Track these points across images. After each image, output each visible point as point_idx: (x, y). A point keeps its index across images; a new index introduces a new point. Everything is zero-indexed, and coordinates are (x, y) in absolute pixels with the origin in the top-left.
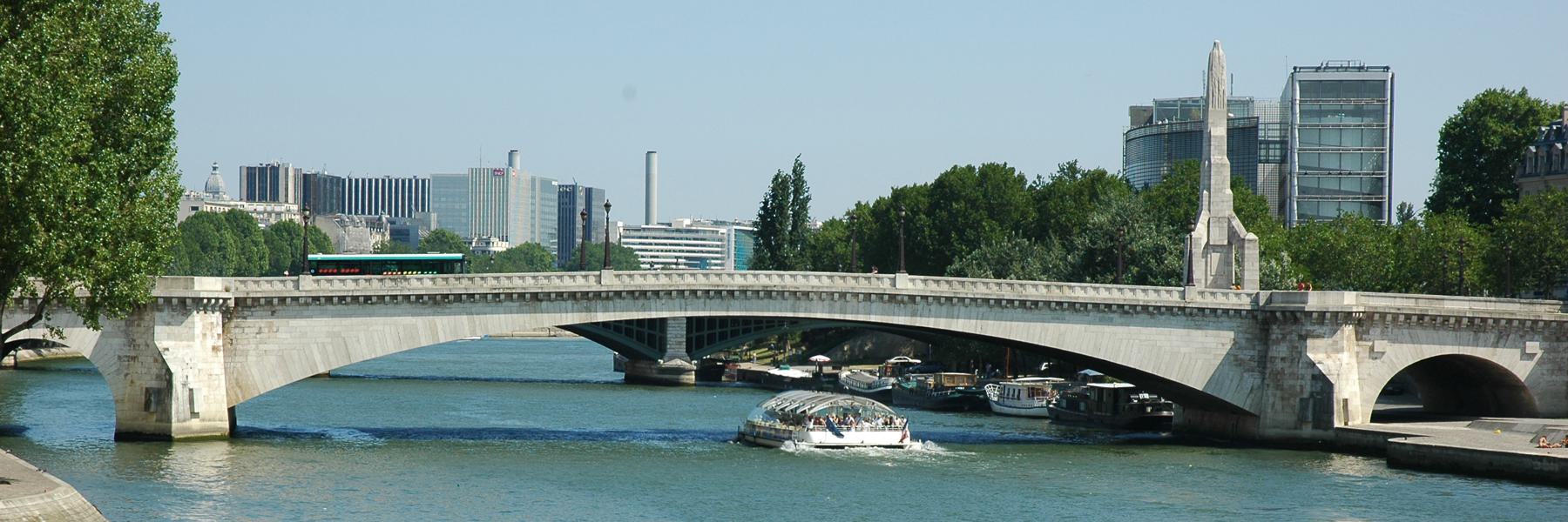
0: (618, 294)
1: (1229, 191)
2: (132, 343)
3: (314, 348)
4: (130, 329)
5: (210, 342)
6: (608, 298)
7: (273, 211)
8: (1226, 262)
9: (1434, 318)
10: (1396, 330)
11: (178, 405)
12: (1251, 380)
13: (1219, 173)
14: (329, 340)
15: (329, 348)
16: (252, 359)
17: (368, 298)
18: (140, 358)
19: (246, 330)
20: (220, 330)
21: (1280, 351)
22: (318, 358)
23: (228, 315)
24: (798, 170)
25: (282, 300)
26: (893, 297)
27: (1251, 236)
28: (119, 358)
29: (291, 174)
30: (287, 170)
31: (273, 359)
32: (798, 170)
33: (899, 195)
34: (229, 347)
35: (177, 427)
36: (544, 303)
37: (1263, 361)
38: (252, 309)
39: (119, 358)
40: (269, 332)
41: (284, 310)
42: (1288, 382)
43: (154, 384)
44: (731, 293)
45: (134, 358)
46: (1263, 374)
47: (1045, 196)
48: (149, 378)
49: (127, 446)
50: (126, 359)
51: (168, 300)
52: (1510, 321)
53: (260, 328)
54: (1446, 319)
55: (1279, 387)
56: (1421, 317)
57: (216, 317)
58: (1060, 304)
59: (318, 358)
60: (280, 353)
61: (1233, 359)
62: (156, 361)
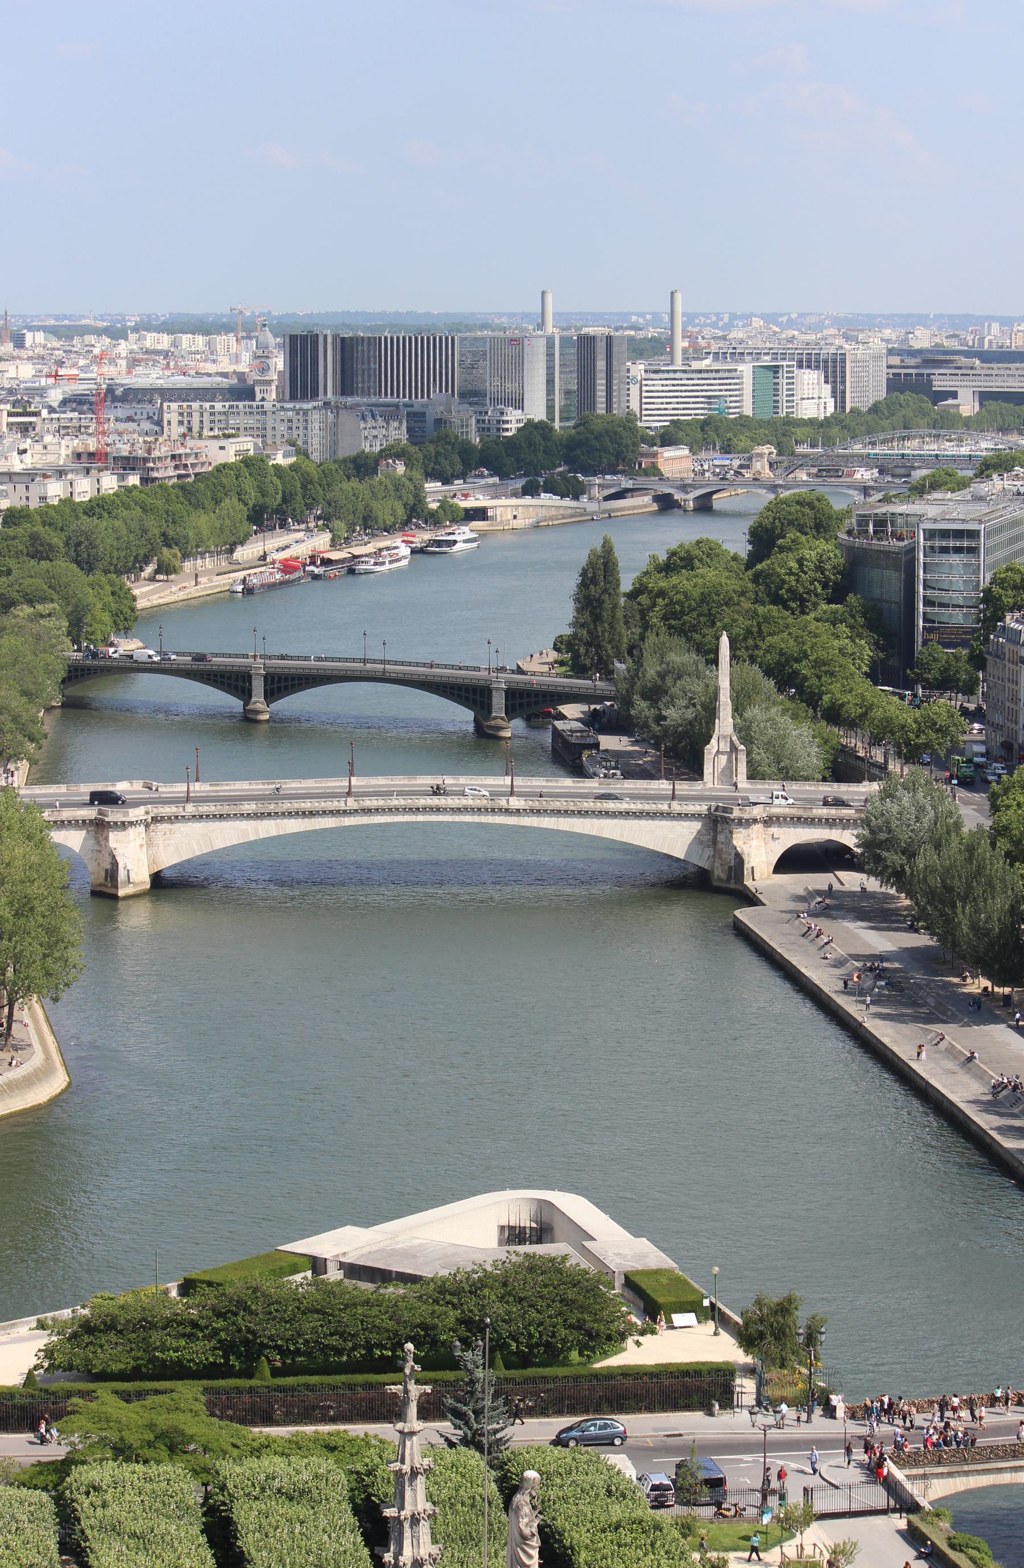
0: (356, 811)
1: (731, 720)
2: (98, 843)
5: (138, 843)
7: (301, 409)
8: (729, 761)
9: (806, 819)
11: (122, 875)
12: (708, 852)
13: (724, 709)
16: (161, 848)
17: (221, 815)
20: (144, 835)
21: (721, 838)
22: (196, 847)
23: (147, 826)
25: (177, 817)
26: (507, 810)
27: (742, 747)
29: (329, 340)
30: (325, 337)
34: (150, 843)
35: (121, 893)
37: (715, 842)
42: (724, 856)
43: (109, 867)
44: (418, 809)
46: (715, 848)
49: (97, 900)
51: (116, 823)
52: (848, 820)
54: (813, 819)
55: (720, 858)
56: (799, 819)
57: (142, 828)
58: (600, 812)
59: (196, 847)
61: (698, 840)
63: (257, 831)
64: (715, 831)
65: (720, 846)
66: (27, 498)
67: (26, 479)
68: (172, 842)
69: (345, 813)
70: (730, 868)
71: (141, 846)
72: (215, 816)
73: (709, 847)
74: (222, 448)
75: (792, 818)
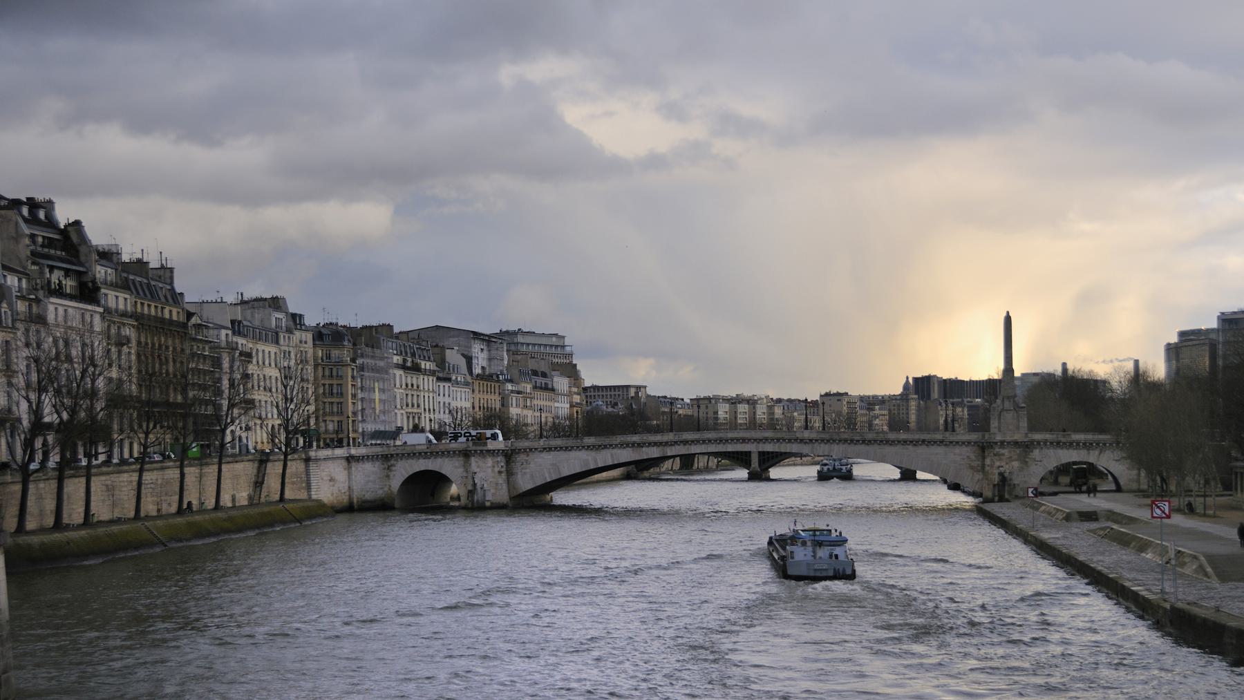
5: (497, 469)
6: (671, 445)
9: (1064, 443)
10: (1046, 450)
12: (979, 476)
15: (552, 471)
16: (519, 476)
17: (567, 448)
22: (547, 475)
34: (510, 473)
36: (644, 449)
37: (983, 466)
56: (1058, 443)
59: (547, 475)
63: (596, 461)
64: (984, 458)
65: (987, 468)
66: (707, 413)
67: (706, 402)
68: (528, 470)
69: (666, 444)
70: (994, 485)
71: (500, 472)
72: (561, 448)
73: (979, 471)
74: (838, 400)
75: (1051, 443)
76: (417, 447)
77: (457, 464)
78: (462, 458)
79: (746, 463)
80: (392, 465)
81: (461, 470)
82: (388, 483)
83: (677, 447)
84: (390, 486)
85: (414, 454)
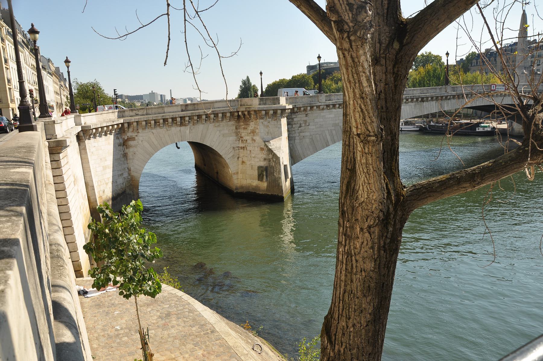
3: (327, 132)
4: (239, 130)
14: (333, 128)
15: (334, 132)
18: (248, 148)
19: (294, 126)
24: (248, 77)
28: (234, 148)
31: (307, 140)
32: (248, 77)
33: (284, 79)
38: (296, 114)
39: (234, 148)
40: (305, 126)
41: (312, 113)
45: (243, 148)
47: (290, 81)
48: (258, 160)
50: (237, 149)
53: (301, 124)
60: (311, 137)
62: (262, 149)
68: (307, 134)
76: (216, 105)
77: (226, 132)
78: (233, 122)
79: (433, 114)
80: (129, 139)
81: (233, 138)
82: (126, 166)
83: (453, 101)
84: (129, 170)
85: (165, 120)
